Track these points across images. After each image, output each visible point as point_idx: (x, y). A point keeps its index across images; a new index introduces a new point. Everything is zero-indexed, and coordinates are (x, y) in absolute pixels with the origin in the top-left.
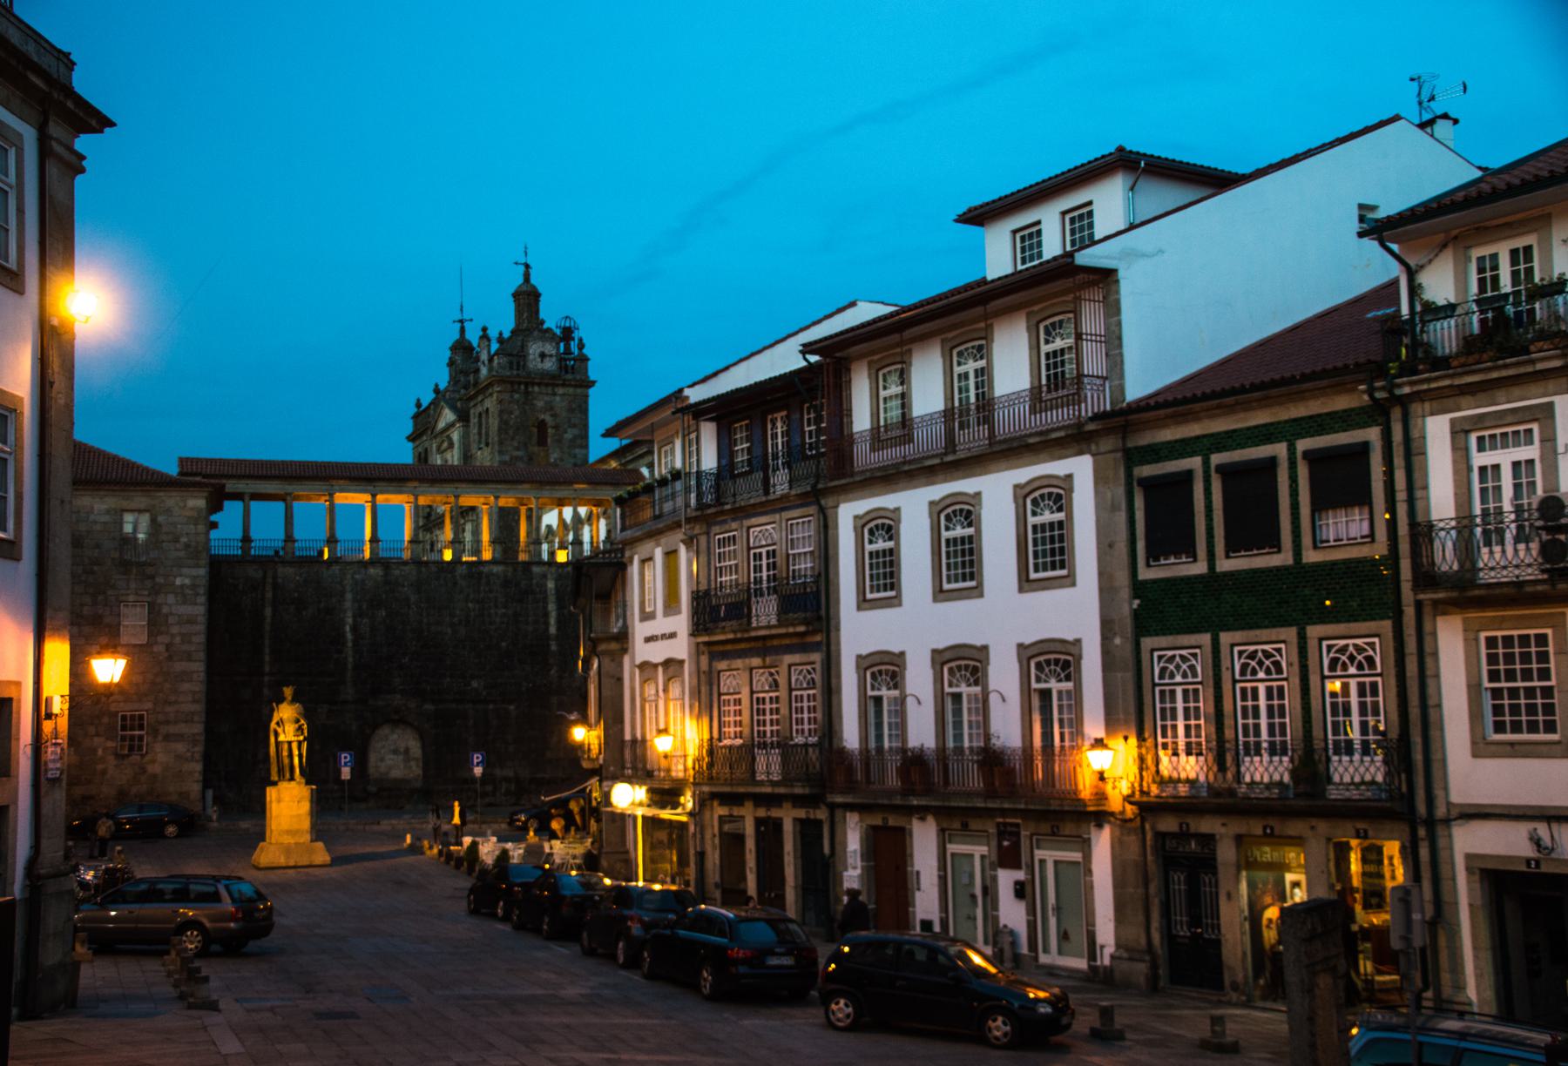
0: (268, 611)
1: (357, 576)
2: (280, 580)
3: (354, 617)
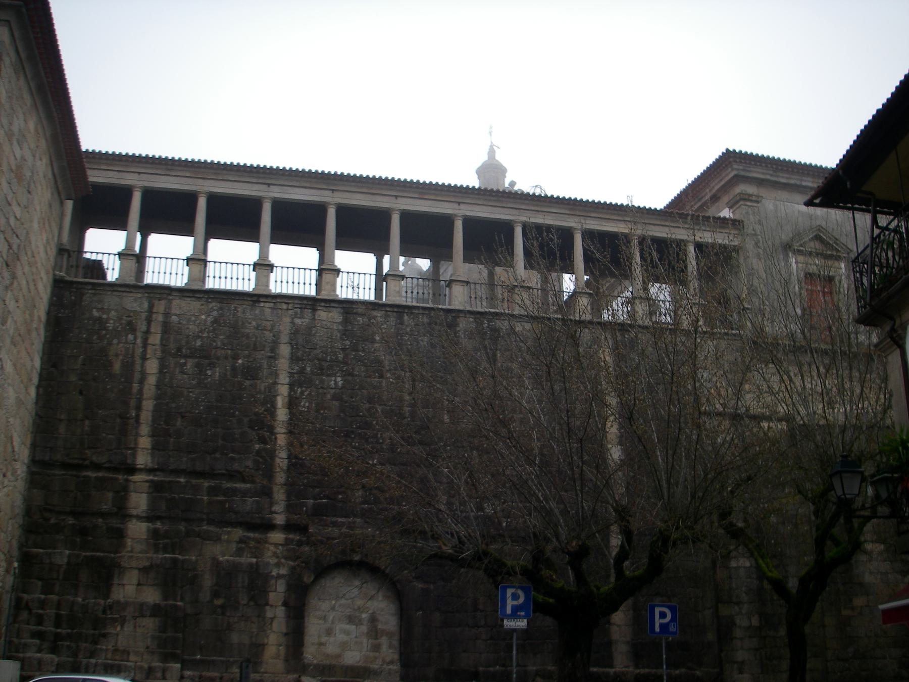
0: (152, 366)
1: (298, 321)
2: (174, 318)
3: (291, 385)
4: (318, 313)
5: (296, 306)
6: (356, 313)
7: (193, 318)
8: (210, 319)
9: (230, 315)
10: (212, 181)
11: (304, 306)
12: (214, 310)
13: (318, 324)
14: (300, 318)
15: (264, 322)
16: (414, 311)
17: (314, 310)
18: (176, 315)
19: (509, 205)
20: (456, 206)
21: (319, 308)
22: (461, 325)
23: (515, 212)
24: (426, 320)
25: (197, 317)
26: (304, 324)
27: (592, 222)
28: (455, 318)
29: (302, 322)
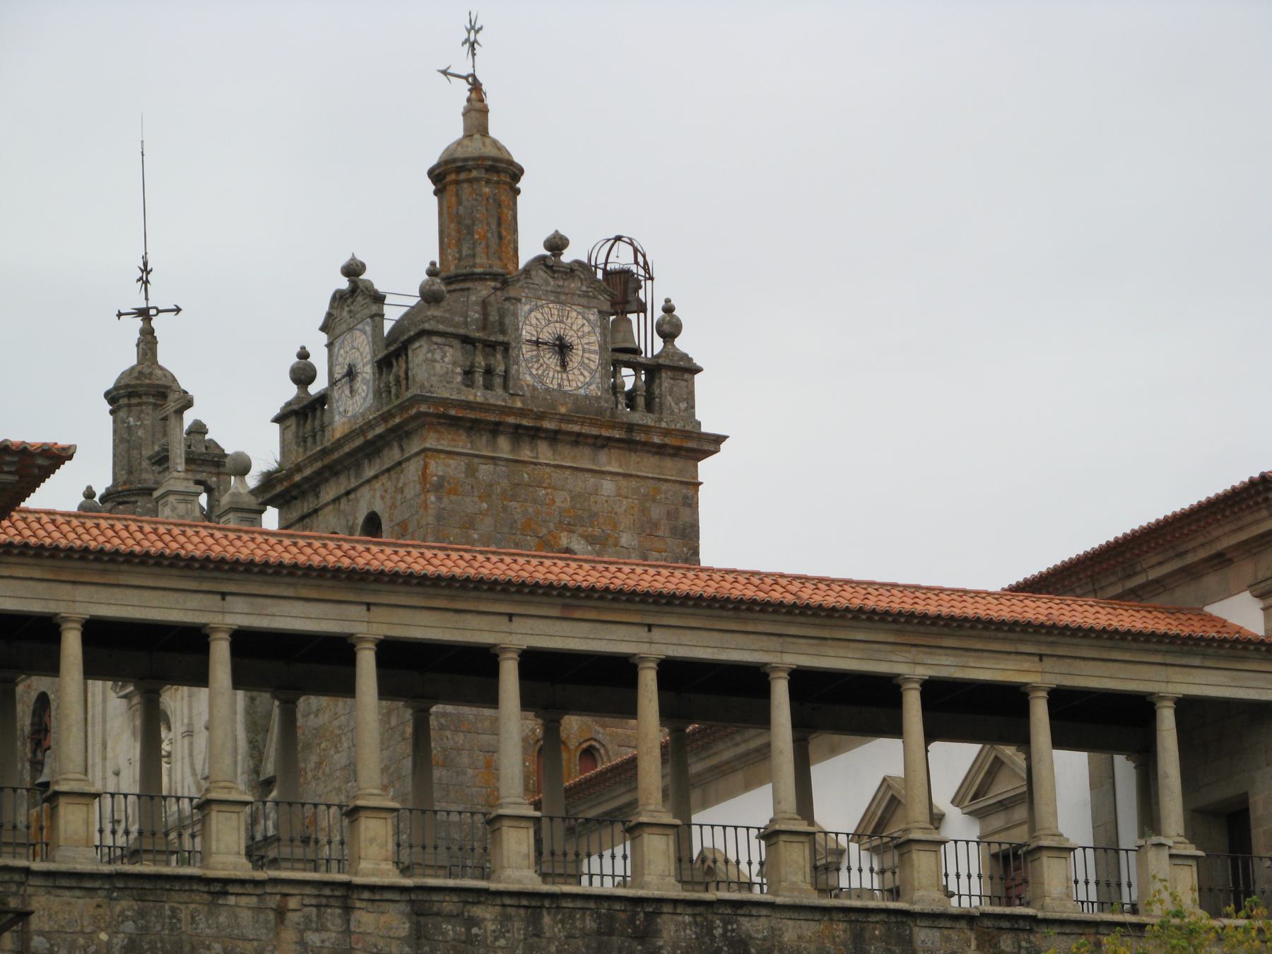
1: (313, 938)
4: (357, 915)
5: (306, 901)
6: (438, 914)
7: (81, 941)
8: (120, 940)
9: (163, 929)
10: (93, 589)
11: (324, 901)
12: (126, 918)
13: (357, 943)
14: (317, 930)
15: (240, 943)
16: (564, 904)
17: (348, 909)
18: (41, 933)
19: (760, 628)
20: (643, 632)
21: (358, 904)
22: (665, 935)
23: (774, 643)
24: (590, 924)
25: (90, 937)
26: (327, 944)
27: (945, 660)
28: (650, 917)
29: (323, 941)
